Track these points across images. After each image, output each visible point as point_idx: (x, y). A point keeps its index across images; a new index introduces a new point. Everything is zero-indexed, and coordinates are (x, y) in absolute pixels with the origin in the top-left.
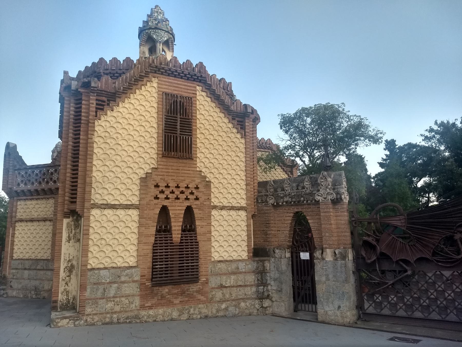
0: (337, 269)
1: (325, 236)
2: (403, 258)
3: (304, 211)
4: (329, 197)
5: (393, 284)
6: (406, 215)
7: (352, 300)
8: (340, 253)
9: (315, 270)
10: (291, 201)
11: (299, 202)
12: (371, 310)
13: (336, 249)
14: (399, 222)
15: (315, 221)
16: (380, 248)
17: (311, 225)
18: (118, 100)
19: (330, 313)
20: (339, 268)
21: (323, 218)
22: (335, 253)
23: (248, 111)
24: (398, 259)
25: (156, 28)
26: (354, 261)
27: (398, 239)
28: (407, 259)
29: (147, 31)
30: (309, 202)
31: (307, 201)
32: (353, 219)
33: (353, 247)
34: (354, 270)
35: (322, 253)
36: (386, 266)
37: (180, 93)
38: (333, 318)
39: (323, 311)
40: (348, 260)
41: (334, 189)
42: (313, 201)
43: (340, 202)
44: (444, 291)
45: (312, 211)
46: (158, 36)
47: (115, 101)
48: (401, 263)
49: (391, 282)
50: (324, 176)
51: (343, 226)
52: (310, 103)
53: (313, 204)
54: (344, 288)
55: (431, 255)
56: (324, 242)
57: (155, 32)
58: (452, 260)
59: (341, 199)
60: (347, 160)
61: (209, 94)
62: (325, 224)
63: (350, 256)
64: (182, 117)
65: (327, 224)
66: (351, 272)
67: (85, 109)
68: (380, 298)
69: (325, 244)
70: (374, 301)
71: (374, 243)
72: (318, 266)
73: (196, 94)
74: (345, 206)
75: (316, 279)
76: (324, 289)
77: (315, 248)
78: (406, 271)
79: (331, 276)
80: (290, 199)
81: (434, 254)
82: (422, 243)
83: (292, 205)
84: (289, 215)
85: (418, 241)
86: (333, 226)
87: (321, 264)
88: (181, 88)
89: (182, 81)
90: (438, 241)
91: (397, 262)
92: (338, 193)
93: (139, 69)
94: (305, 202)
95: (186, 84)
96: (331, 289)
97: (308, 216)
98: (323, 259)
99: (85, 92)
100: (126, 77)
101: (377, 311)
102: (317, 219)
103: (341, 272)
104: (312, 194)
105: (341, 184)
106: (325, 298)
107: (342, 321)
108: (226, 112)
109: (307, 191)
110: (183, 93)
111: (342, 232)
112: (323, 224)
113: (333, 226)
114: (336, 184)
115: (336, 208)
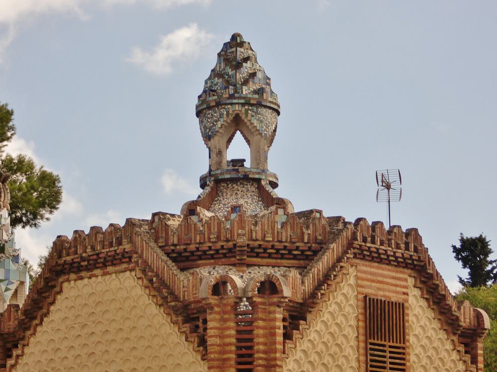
18: (309, 317)
23: (486, 327)
25: (259, 105)
29: (237, 107)
37: (387, 294)
46: (261, 122)
47: (305, 319)
57: (257, 113)
61: (425, 292)
64: (391, 344)
67: (265, 336)
73: (407, 294)
88: (387, 284)
89: (389, 270)
93: (335, 253)
95: (394, 274)
99: (264, 304)
100: (319, 270)
108: (449, 329)
110: (391, 295)
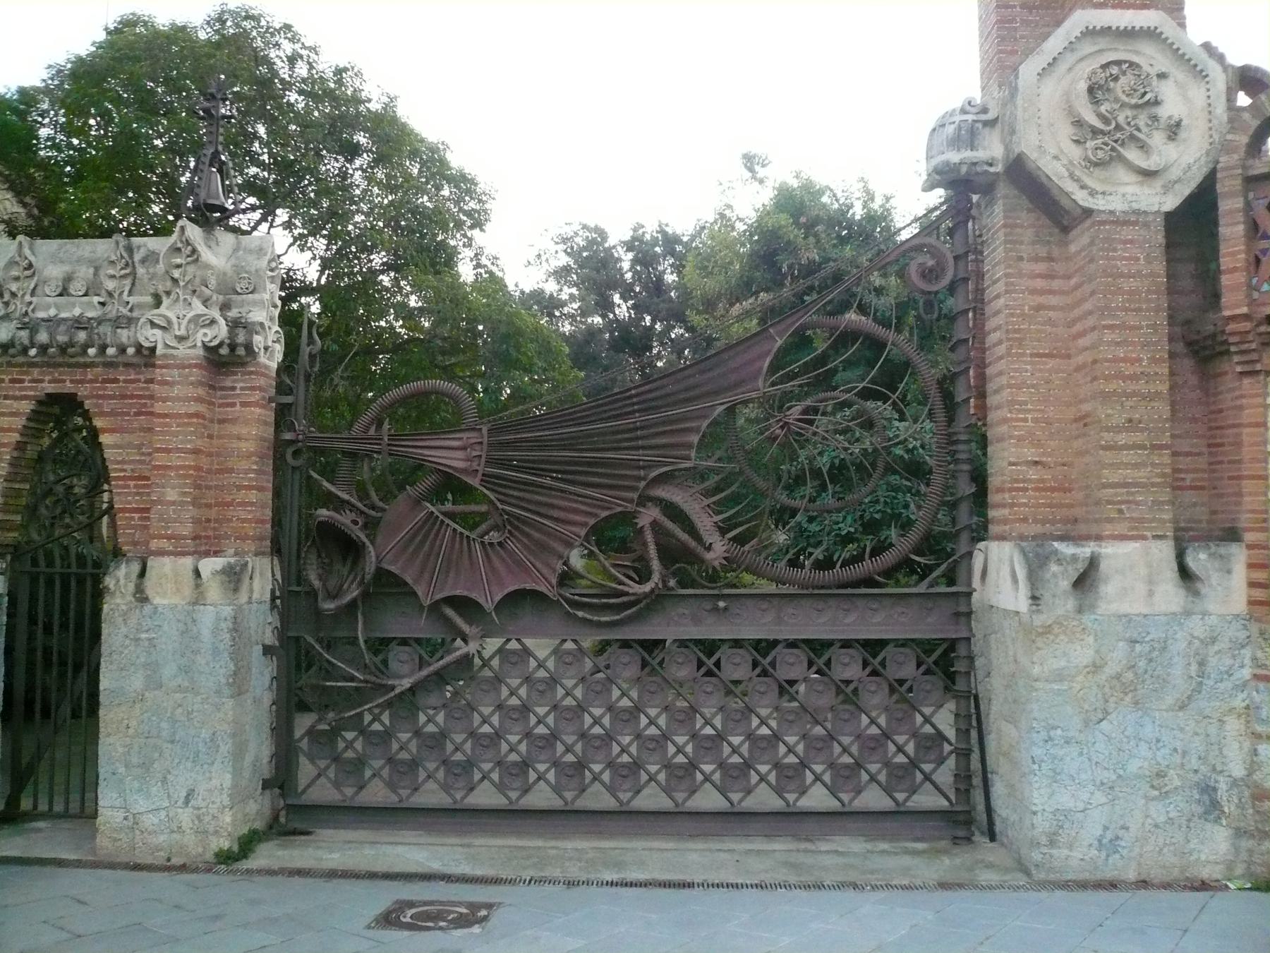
0: (196, 638)
1: (159, 502)
2: (458, 592)
3: (82, 391)
5: (412, 690)
6: (485, 430)
7: (249, 759)
9: (103, 648)
10: (26, 342)
11: (63, 349)
12: (323, 792)
14: (460, 454)
15: (128, 438)
16: (377, 557)
17: (108, 453)
19: (150, 821)
20: (206, 633)
21: (161, 425)
22: (197, 573)
24: (438, 597)
26: (273, 606)
27: (447, 521)
28: (473, 595)
30: (111, 351)
31: (103, 348)
32: (288, 436)
34: (268, 642)
35: (142, 574)
36: (396, 624)
38: (162, 838)
39: (120, 815)
40: (250, 602)
41: (225, 307)
42: (131, 351)
43: (243, 364)
44: (581, 708)
45: (124, 397)
48: (450, 612)
49: (407, 683)
50: (188, 243)
51: (244, 465)
53: (127, 365)
54: (221, 715)
55: (554, 581)
56: (155, 525)
58: (625, 599)
59: (249, 347)
62: (168, 451)
65: (178, 450)
66: (258, 649)
68: (358, 745)
69: (161, 537)
70: (336, 759)
71: (360, 534)
75: (105, 683)
76: (134, 723)
79: (168, 671)
80: (24, 334)
82: (528, 536)
83: (33, 365)
84: (15, 404)
85: (517, 528)
87: (133, 621)
90: (583, 532)
91: (435, 606)
92: (235, 324)
94: (92, 351)
96: (164, 725)
97: (102, 414)
98: (141, 597)
101: (341, 792)
102: (142, 429)
103: (216, 652)
106: (135, 760)
107: (200, 850)
109: (108, 308)
111: (240, 488)
112: (159, 450)
115: (222, 389)
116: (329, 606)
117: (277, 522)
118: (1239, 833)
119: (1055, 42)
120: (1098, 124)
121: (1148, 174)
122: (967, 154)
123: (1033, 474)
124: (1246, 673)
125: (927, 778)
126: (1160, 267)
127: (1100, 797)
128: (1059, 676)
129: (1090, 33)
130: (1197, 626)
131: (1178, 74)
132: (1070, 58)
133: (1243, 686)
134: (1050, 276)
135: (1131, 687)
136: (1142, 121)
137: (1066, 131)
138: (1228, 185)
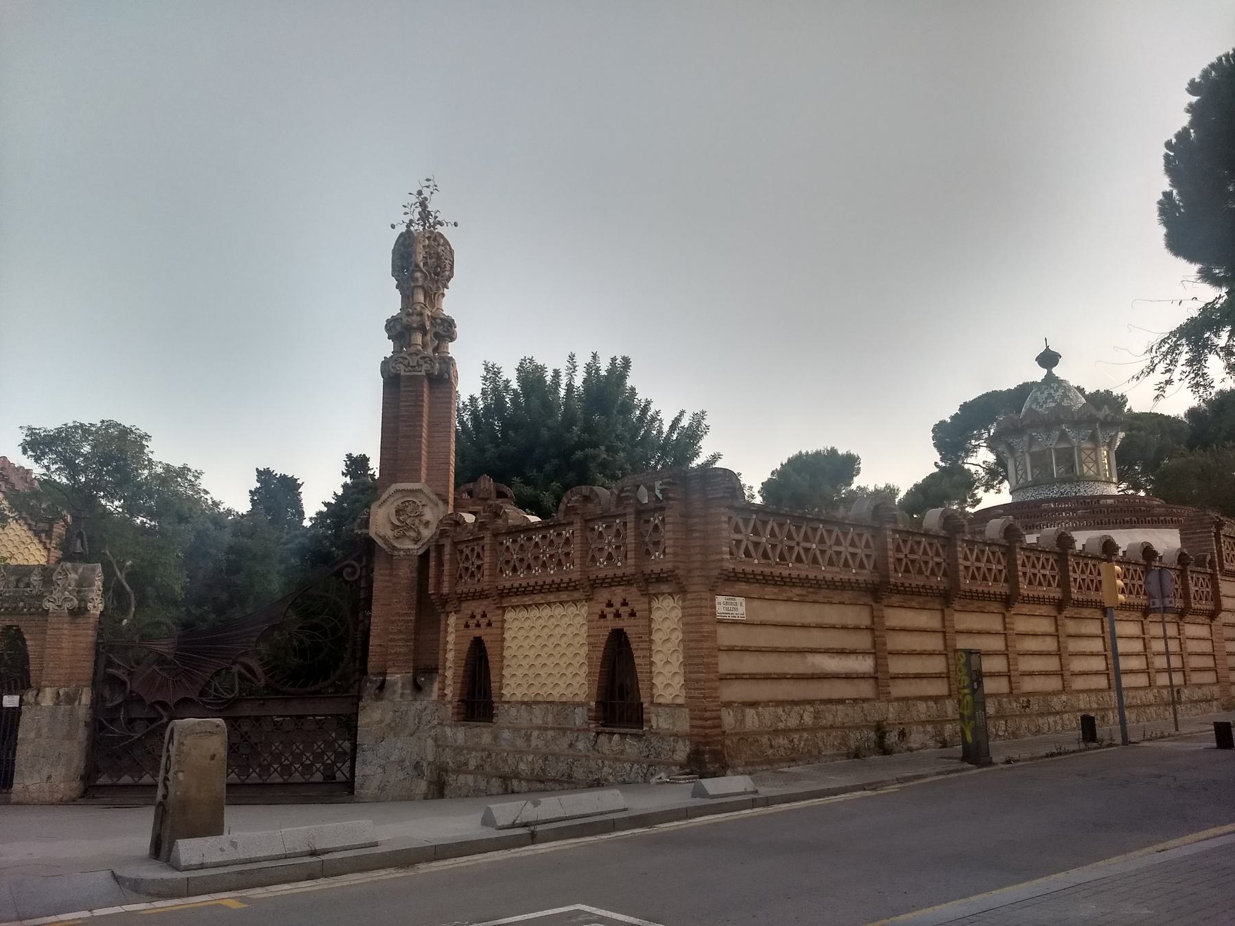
4: (67, 605)
8: (67, 694)
12: (103, 780)
13: (61, 687)
17: (29, 648)
33: (94, 684)
41: (79, 592)
52: (92, 417)
60: (258, 485)
63: (86, 698)
66: (82, 724)
72: (25, 719)
74: (91, 620)
77: (29, 686)
78: (161, 718)
81: (202, 693)
86: (65, 652)
91: (152, 705)
104: (40, 597)
105: (91, 584)
113: (65, 652)
114: (83, 583)
116: (109, 705)
117: (95, 674)
118: (430, 783)
119: (384, 496)
120: (397, 523)
121: (416, 541)
122: (364, 531)
123: (378, 649)
124: (436, 722)
125: (339, 769)
126: (415, 575)
127: (380, 770)
128: (368, 725)
129: (397, 491)
130: (418, 705)
131: (431, 505)
132: (392, 499)
133: (434, 727)
134: (390, 575)
135: (394, 729)
136: (417, 522)
137: (389, 526)
138: (432, 548)
